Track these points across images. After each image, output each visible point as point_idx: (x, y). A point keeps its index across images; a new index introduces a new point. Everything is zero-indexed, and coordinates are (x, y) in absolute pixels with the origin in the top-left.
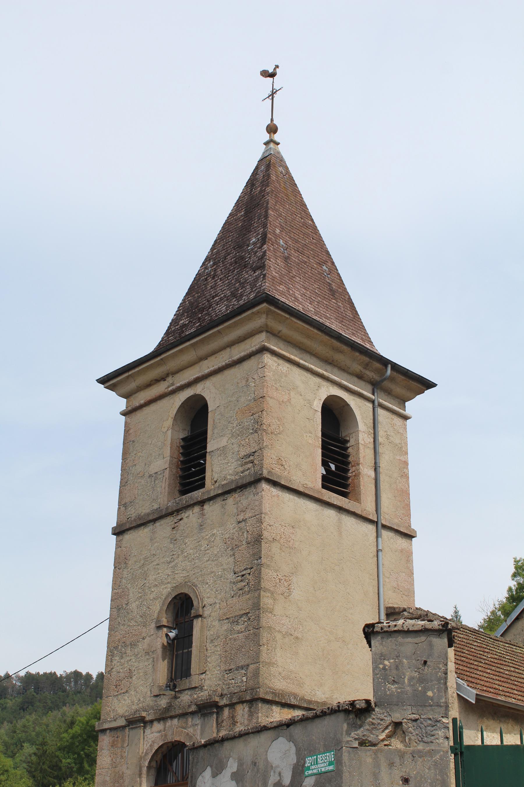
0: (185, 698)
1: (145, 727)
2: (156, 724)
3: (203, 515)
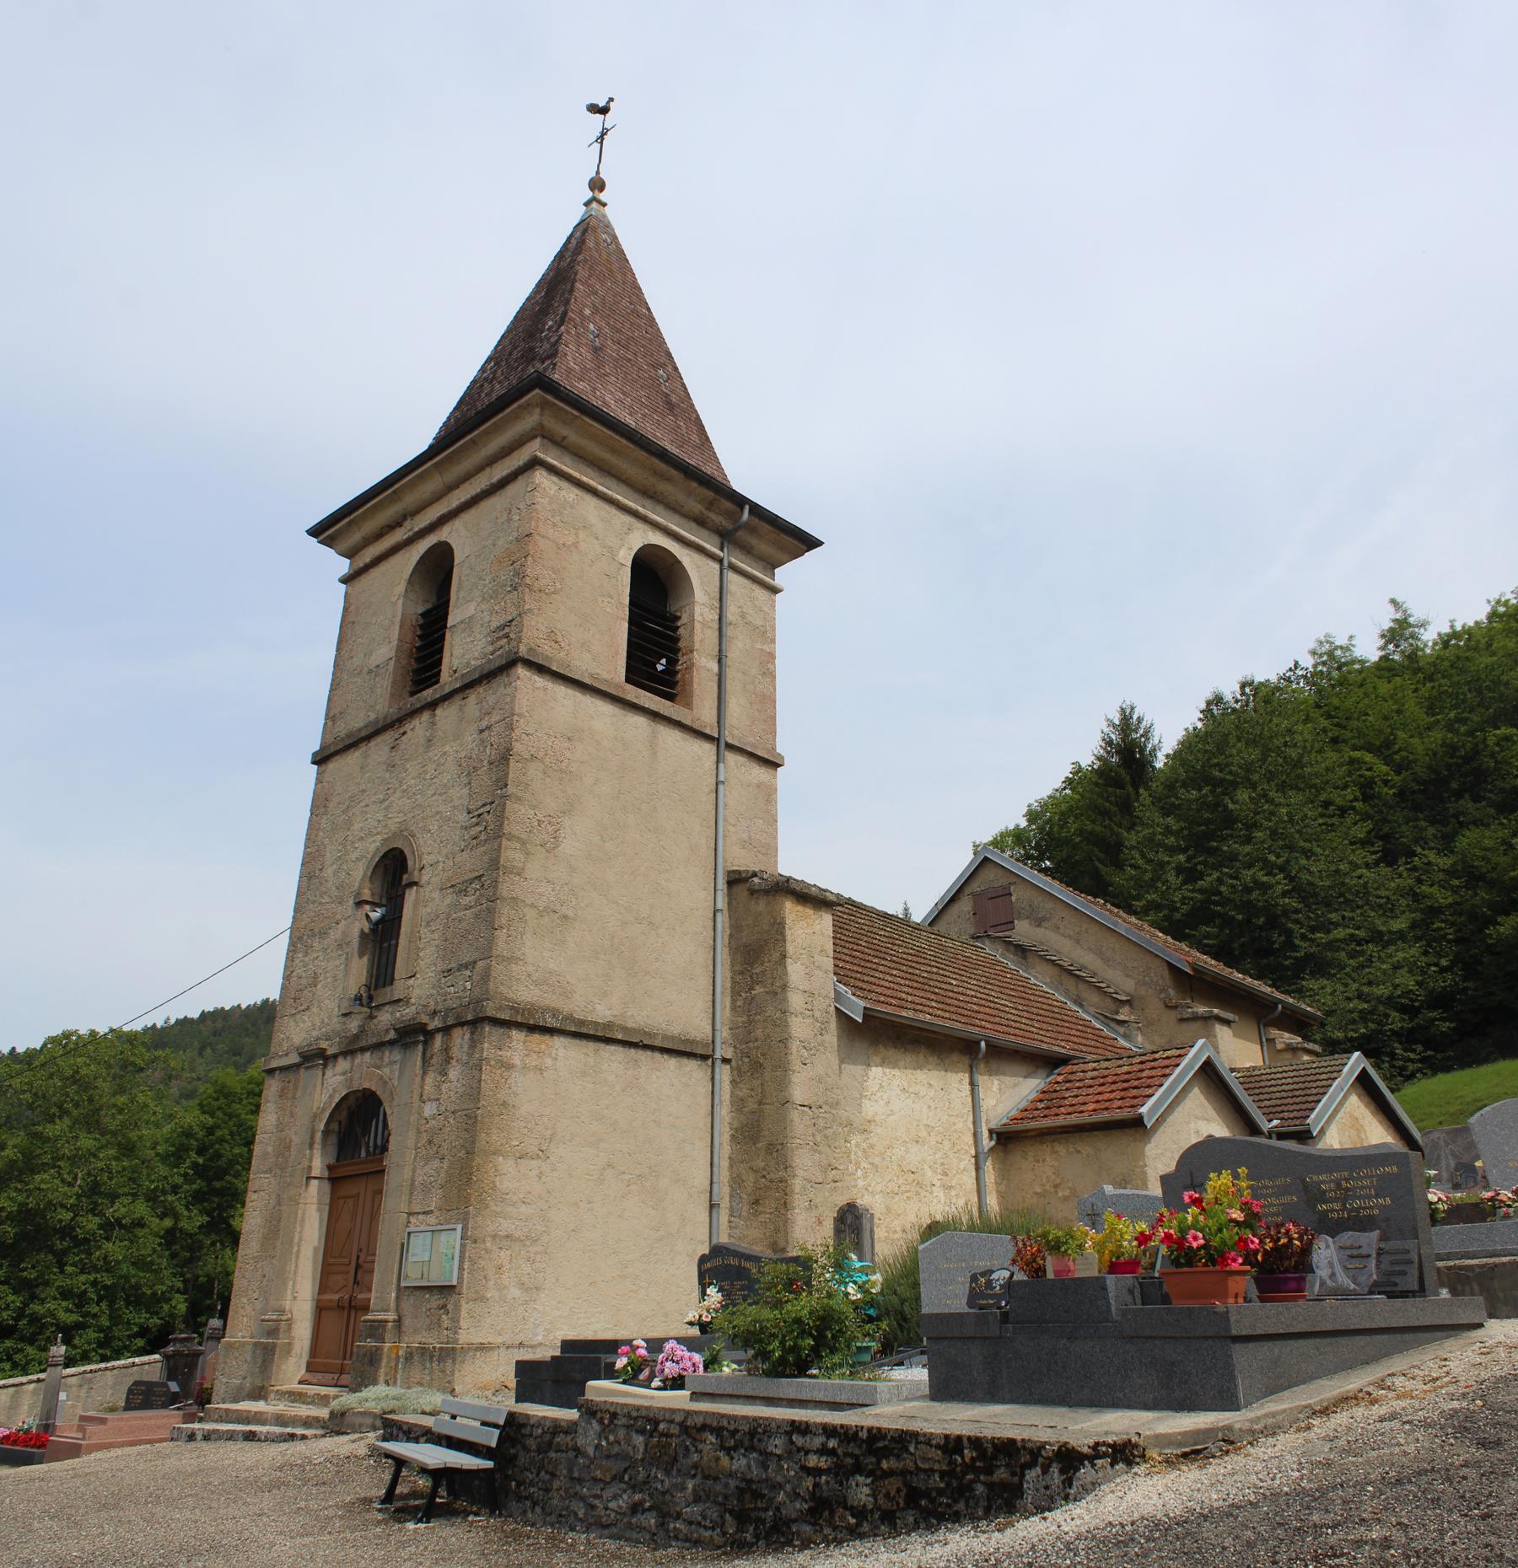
0: (385, 1018)
1: (325, 1066)
2: (341, 1060)
3: (434, 724)
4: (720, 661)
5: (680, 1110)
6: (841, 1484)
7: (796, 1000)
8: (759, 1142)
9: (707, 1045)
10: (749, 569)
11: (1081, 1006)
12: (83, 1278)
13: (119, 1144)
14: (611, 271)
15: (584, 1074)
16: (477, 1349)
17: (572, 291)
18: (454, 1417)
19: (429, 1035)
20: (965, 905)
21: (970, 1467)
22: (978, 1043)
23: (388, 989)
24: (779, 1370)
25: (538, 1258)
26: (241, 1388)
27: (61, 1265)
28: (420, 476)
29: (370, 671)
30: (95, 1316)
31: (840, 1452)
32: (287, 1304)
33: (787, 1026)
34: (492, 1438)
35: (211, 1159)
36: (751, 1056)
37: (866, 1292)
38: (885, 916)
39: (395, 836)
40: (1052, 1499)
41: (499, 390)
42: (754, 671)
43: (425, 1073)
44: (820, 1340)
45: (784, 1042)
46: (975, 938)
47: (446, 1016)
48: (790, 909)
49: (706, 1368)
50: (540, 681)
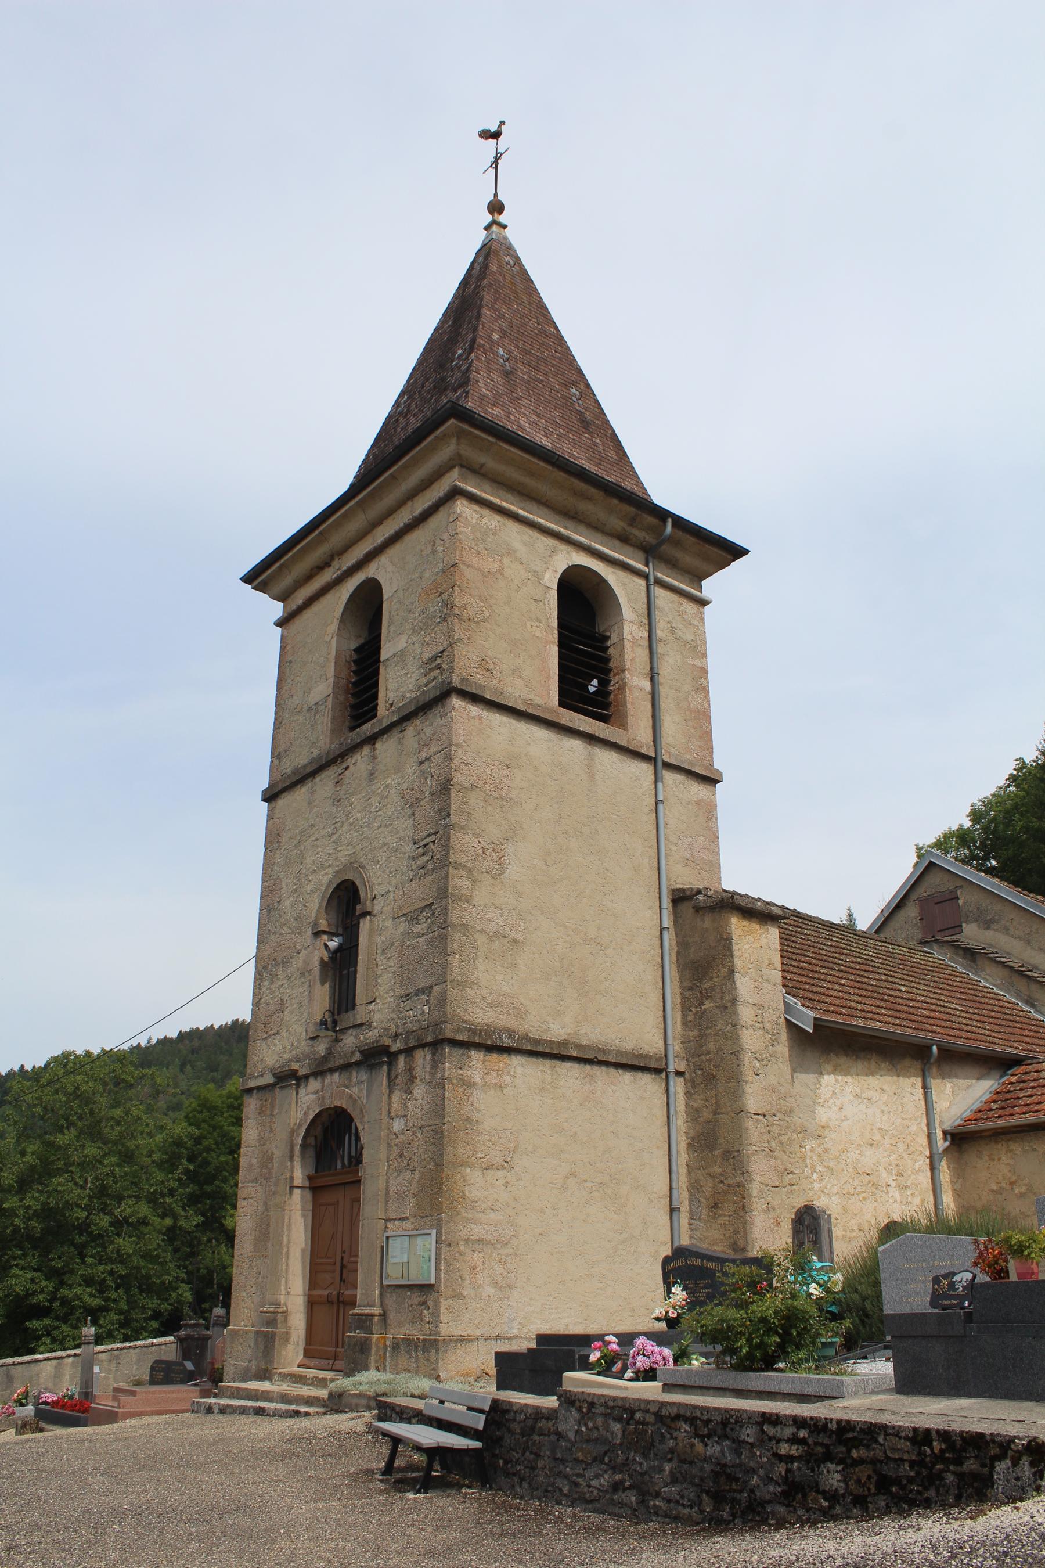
0: (349, 1041)
1: (298, 1085)
3: (374, 757)
4: (652, 679)
5: (639, 1119)
6: (813, 1470)
7: (746, 1013)
8: (715, 1150)
9: (659, 1059)
10: (676, 583)
11: (1033, 1006)
12: (101, 1268)
13: (120, 1152)
14: (515, 293)
15: (542, 1090)
16: (457, 1341)
17: (479, 316)
18: (442, 1402)
19: (393, 1056)
20: (912, 911)
21: (939, 1458)
22: (930, 1048)
23: (350, 1013)
24: (746, 1365)
25: (509, 1259)
26: (247, 1369)
27: (82, 1256)
28: (345, 516)
29: (310, 709)
30: (115, 1300)
31: (810, 1441)
32: (282, 1299)
33: (738, 1038)
34: (479, 1422)
35: (200, 1166)
36: (704, 1070)
37: (828, 1291)
38: (830, 926)
39: (346, 868)
40: (1023, 1490)
41: (414, 423)
42: (687, 688)
43: (391, 1092)
44: (786, 1337)
45: (736, 1054)
46: (922, 943)
47: (407, 1039)
48: (736, 925)
49: (675, 1361)
50: (474, 710)
